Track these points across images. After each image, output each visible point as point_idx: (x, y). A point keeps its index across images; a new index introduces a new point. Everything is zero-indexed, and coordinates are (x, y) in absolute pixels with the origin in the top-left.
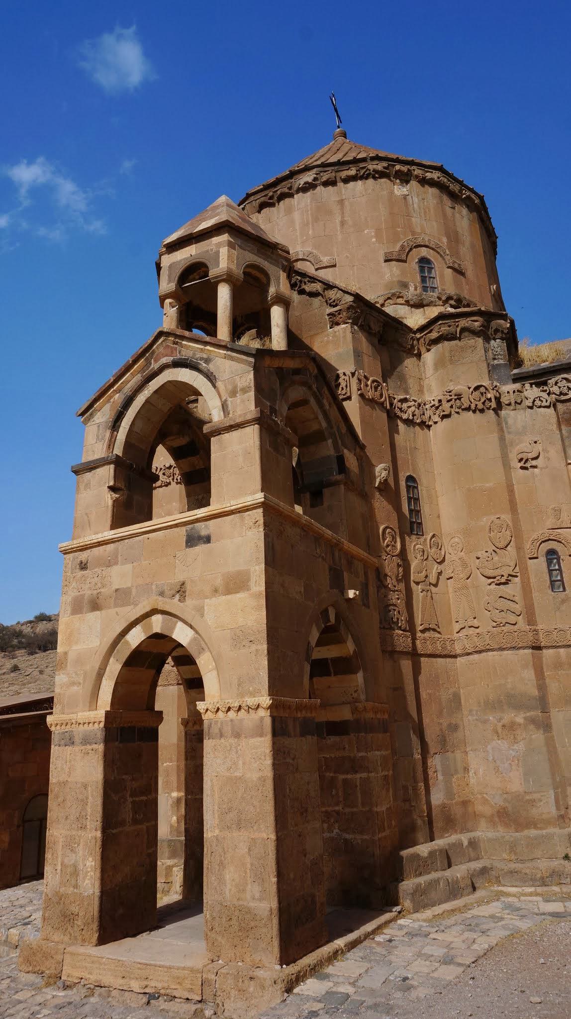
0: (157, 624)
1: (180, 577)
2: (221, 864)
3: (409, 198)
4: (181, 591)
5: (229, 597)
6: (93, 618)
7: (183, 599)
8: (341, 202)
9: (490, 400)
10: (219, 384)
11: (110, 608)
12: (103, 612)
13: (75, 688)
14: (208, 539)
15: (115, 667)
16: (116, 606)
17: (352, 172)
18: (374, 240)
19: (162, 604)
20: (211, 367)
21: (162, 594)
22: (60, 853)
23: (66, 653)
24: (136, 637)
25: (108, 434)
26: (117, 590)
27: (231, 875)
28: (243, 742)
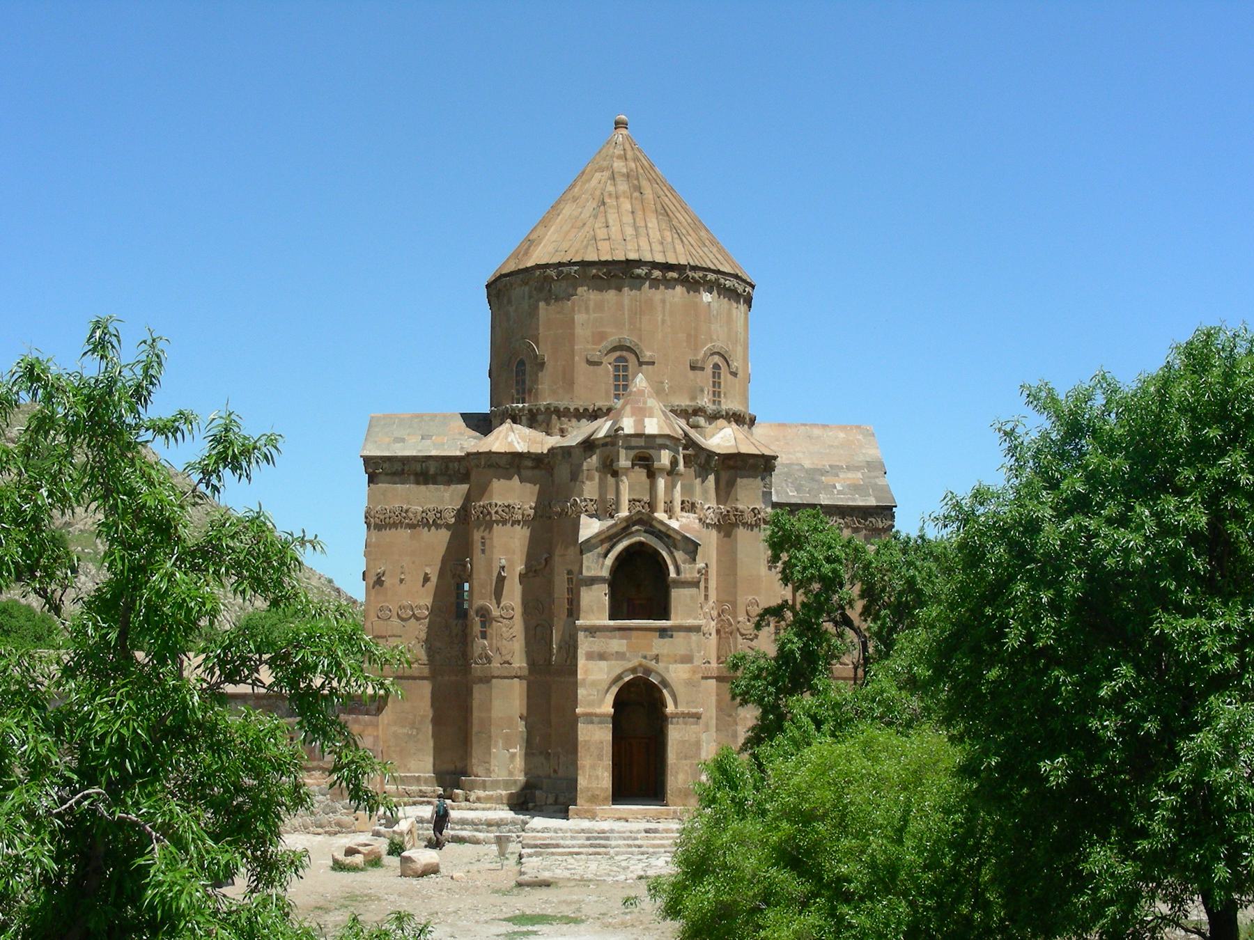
1: (655, 652)
2: (676, 772)
3: (711, 304)
4: (657, 658)
5: (682, 665)
6: (603, 664)
7: (657, 662)
8: (663, 301)
9: (760, 519)
11: (612, 660)
12: (609, 662)
13: (592, 697)
14: (672, 637)
15: (615, 690)
16: (617, 660)
17: (675, 275)
18: (685, 344)
21: (645, 657)
22: (587, 770)
23: (584, 680)
26: (617, 652)
27: (681, 777)
28: (688, 726)
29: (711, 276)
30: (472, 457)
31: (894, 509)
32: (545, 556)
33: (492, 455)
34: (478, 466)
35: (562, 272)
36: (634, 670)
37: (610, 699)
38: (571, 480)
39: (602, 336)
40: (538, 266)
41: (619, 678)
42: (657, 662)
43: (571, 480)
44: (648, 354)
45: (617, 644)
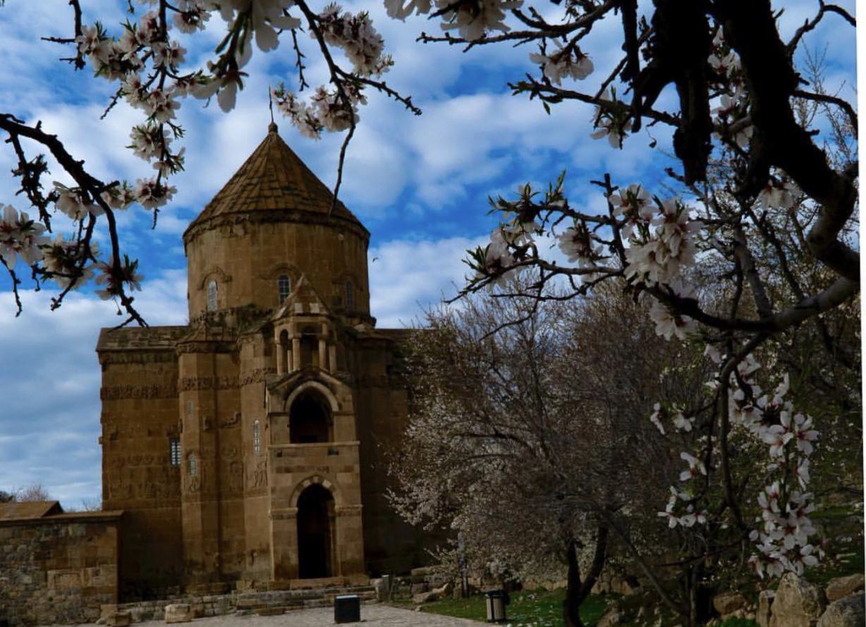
0: (316, 480)
6: (289, 475)
7: (328, 472)
10: (337, 395)
15: (298, 494)
19: (319, 473)
21: (319, 469)
24: (307, 484)
25: (283, 402)
29: (343, 223)
32: (236, 413)
34: (184, 352)
35: (238, 218)
36: (311, 478)
37: (295, 501)
38: (255, 356)
39: (271, 261)
41: (300, 484)
42: (328, 472)
43: (255, 356)
45: (297, 461)
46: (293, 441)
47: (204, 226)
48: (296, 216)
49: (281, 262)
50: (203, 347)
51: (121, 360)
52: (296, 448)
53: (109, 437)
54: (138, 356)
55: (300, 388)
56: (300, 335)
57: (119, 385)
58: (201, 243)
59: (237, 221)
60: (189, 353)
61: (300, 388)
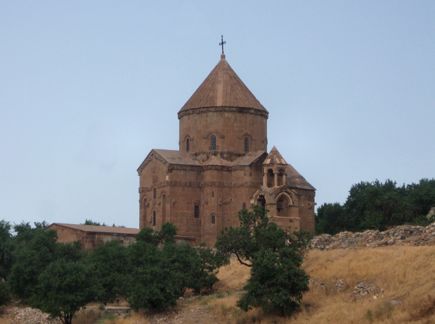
1: (289, 226)
20: (291, 195)
30: (209, 166)
31: (315, 191)
33: (217, 166)
35: (230, 109)
38: (244, 175)
40: (222, 107)
44: (254, 138)
46: (278, 216)
47: (210, 109)
48: (252, 111)
49: (245, 132)
50: (219, 168)
51: (178, 169)
52: (279, 218)
53: (173, 203)
54: (184, 168)
55: (280, 194)
56: (278, 172)
57: (176, 180)
58: (207, 116)
59: (229, 111)
60: (213, 170)
61: (280, 194)
